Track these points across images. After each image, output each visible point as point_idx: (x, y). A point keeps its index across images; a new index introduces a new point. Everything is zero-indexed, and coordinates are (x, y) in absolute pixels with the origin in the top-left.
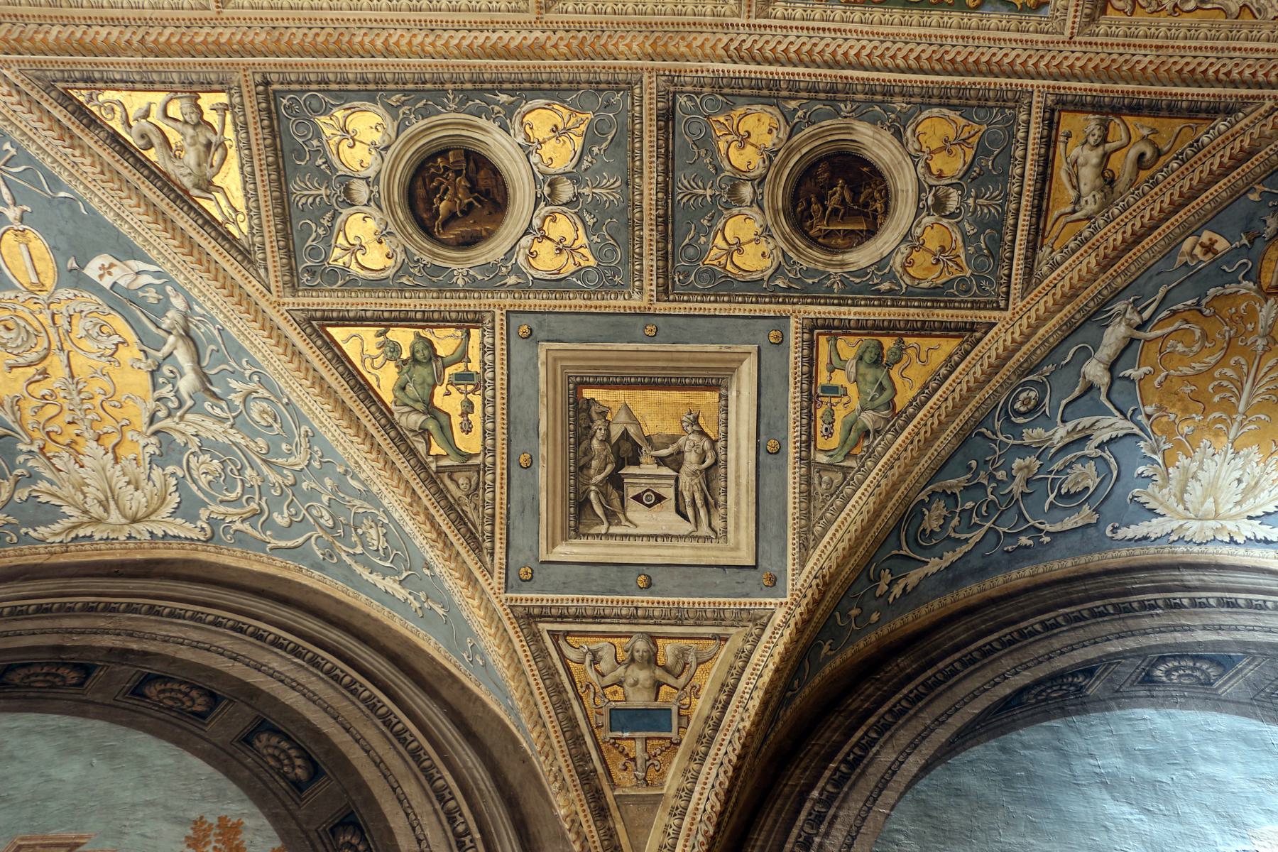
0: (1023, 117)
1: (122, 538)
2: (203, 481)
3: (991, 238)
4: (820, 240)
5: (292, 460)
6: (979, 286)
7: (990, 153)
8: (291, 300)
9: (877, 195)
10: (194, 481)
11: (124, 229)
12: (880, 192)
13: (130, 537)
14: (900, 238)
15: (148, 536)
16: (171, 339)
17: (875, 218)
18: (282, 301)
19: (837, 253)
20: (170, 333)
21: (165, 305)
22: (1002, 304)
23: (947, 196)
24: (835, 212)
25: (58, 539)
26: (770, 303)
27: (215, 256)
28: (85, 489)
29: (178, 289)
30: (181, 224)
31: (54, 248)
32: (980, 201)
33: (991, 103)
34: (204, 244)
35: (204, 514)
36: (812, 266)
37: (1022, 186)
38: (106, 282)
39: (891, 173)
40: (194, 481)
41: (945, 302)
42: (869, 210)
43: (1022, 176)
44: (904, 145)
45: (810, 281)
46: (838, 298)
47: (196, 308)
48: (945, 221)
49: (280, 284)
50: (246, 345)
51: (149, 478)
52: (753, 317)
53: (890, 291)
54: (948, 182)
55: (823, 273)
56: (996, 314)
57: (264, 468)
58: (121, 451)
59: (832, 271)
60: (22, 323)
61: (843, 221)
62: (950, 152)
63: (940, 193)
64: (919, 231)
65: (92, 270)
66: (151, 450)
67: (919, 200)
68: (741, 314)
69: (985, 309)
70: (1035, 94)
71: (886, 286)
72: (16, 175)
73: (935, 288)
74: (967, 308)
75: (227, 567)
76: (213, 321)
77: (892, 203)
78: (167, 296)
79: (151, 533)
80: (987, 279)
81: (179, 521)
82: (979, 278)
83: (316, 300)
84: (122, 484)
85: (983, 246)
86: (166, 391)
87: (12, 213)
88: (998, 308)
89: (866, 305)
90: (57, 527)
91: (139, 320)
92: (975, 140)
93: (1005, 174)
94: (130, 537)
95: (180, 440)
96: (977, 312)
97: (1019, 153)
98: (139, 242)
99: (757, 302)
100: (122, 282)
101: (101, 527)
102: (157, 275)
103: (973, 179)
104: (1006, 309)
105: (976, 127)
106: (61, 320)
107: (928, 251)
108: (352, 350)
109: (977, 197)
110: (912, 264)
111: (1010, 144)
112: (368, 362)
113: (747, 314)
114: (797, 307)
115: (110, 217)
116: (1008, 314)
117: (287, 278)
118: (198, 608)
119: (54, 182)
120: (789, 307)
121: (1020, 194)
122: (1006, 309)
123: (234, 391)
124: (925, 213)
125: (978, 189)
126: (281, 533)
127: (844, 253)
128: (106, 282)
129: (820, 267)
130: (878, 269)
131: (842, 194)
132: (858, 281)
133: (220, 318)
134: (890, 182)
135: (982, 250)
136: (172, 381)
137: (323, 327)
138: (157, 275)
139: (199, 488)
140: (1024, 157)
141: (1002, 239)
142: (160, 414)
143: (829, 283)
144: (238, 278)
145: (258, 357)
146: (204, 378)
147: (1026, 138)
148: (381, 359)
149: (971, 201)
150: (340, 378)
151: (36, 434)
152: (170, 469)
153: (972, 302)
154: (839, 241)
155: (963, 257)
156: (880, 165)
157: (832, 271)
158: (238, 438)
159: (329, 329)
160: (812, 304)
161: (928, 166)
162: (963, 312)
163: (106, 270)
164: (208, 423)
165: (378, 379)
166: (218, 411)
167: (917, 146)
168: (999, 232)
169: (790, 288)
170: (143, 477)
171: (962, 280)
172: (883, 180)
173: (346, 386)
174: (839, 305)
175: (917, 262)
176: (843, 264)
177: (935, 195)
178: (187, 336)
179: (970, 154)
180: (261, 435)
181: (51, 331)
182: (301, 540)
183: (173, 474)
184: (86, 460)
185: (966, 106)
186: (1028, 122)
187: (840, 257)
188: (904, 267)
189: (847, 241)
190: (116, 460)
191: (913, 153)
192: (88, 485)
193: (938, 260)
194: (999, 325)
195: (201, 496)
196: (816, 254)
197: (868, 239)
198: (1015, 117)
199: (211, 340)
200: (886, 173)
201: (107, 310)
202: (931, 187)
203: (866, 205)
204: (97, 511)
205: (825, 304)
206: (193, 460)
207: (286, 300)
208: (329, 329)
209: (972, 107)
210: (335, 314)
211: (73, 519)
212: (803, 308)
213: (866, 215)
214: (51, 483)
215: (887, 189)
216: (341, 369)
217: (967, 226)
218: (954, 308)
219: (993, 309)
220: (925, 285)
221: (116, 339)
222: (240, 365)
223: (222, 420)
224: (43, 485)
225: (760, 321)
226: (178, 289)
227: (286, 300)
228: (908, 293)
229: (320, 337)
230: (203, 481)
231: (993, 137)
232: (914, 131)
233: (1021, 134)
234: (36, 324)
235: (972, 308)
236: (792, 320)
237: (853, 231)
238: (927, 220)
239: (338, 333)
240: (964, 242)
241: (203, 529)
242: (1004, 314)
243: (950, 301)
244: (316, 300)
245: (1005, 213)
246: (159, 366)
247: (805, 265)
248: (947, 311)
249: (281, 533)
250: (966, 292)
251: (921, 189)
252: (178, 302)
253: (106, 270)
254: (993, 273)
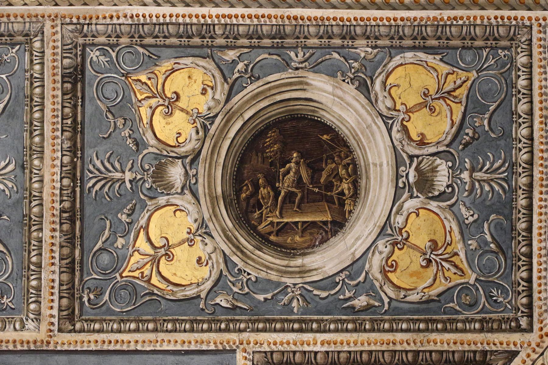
0: (522, 59)
3: (498, 226)
4: (272, 238)
6: (489, 297)
7: (484, 109)
9: (342, 172)
12: (346, 167)
14: (377, 231)
17: (342, 204)
19: (294, 256)
22: (524, 322)
23: (434, 170)
24: (290, 196)
26: (210, 330)
32: (478, 175)
33: (479, 43)
36: (263, 275)
37: (531, 152)
39: (359, 141)
41: (443, 322)
42: (334, 193)
43: (531, 138)
44: (373, 103)
45: (261, 297)
46: (299, 321)
48: (433, 205)
52: (188, 352)
53: (368, 308)
54: (433, 150)
55: (278, 284)
56: (516, 337)
59: (289, 281)
61: (301, 210)
62: (432, 110)
63: (424, 166)
64: (400, 220)
67: (398, 177)
68: (171, 347)
69: (500, 330)
70: (535, 28)
71: (361, 301)
73: (429, 301)
74: (475, 331)
77: (363, 182)
80: (499, 286)
82: (487, 285)
85: (489, 238)
88: (519, 329)
89: (336, 331)
92: (462, 92)
93: (506, 135)
96: (490, 336)
97: (522, 107)
99: (192, 330)
103: (466, 145)
104: (530, 329)
105: (463, 75)
107: (415, 247)
109: (473, 170)
110: (394, 267)
111: (508, 96)
113: (179, 347)
114: (245, 336)
116: (533, 337)
120: (234, 336)
121: (530, 162)
122: (530, 329)
124: (406, 195)
125: (473, 159)
127: (304, 255)
129: (274, 276)
130: (351, 278)
131: (297, 172)
132: (324, 294)
134: (358, 153)
135: (487, 243)
140: (531, 113)
141: (513, 228)
143: (286, 299)
147: (530, 87)
149: (465, 176)
153: (481, 321)
154: (297, 238)
155: (462, 255)
156: (344, 131)
157: (289, 281)
160: (264, 330)
161: (405, 130)
162: (469, 336)
167: (389, 103)
168: (508, 217)
169: (235, 308)
171: (465, 288)
172: (350, 151)
174: (301, 330)
175: (402, 265)
176: (303, 271)
177: (417, 169)
179: (458, 111)
185: (448, 48)
186: (530, 66)
187: (299, 261)
188: (384, 272)
189: (308, 238)
191: (385, 112)
193: (429, 261)
194: (522, 355)
196: (268, 258)
197: (335, 233)
198: (512, 61)
200: (352, 142)
202: (411, 157)
203: (329, 186)
205: (283, 330)
209: (455, 48)
212: (253, 337)
213: (330, 200)
215: (354, 163)
217: (463, 210)
218: (457, 331)
219: (512, 330)
220: (414, 297)
225: (196, 358)
228: (393, 311)
231: (485, 88)
232: (384, 83)
233: (522, 82)
235: (481, 330)
236: (239, 355)
237: (313, 224)
238: (410, 204)
240: (462, 233)
242: (528, 337)
243: (452, 321)
245: (513, 190)
247: (254, 274)
248: (447, 336)
250: (472, 306)
251: (398, 162)
254: (506, 276)
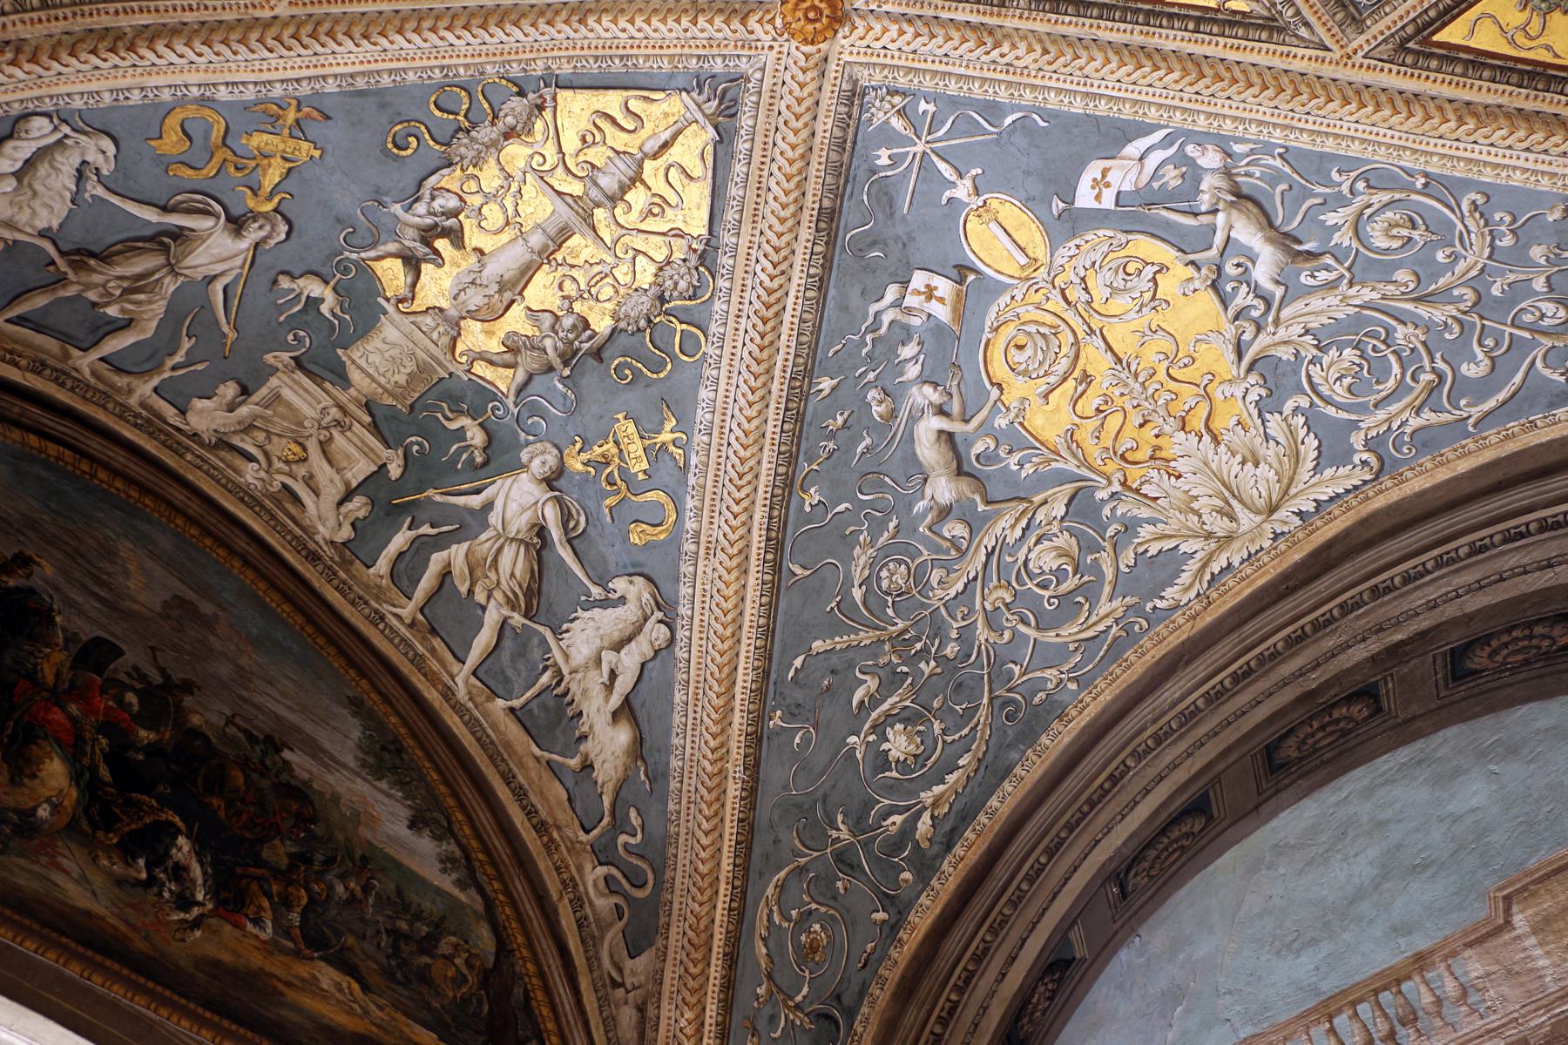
1: (1267, 544)
2: (1340, 392)
5: (1461, 267)
8: (1362, 39)
10: (1327, 401)
11: (1102, 109)
13: (1276, 536)
15: (1297, 521)
16: (1221, 218)
18: (1349, 50)
20: (1215, 212)
21: (1193, 173)
25: (1192, 594)
27: (1232, 56)
28: (1195, 505)
29: (1201, 139)
30: (1170, 46)
31: (1028, 202)
34: (1209, 51)
35: (1357, 440)
38: (1108, 202)
40: (1327, 401)
47: (1238, 148)
49: (1336, 29)
50: (1330, 146)
51: (1267, 437)
57: (1423, 311)
58: (1216, 425)
60: (1032, 328)
65: (1085, 198)
66: (1253, 396)
72: (948, 136)
75: (1421, 495)
76: (1268, 148)
78: (1191, 162)
79: (1300, 514)
81: (1329, 472)
83: (1394, 16)
84: (1236, 469)
86: (1242, 298)
87: (962, 191)
90: (1185, 578)
91: (1169, 224)
94: (1276, 536)
95: (1285, 354)
98: (1127, 113)
100: (1127, 187)
101: (1236, 545)
102: (1167, 142)
106: (1075, 294)
108: (1487, 40)
112: (1520, 39)
115: (1078, 107)
117: (1339, 16)
118: (1435, 552)
119: (992, 110)
123: (1336, 227)
126: (1481, 388)
128: (1108, 202)
133: (1277, 136)
136: (1245, 278)
137: (1426, 41)
138: (1167, 142)
139: (1338, 407)
142: (1247, 337)
144: (1277, 62)
145: (1355, 150)
146: (1285, 241)
148: (1536, 22)
150: (1493, 86)
151: (1111, 467)
152: (1289, 406)
158: (1368, 295)
159: (1436, 38)
163: (1100, 184)
164: (1316, 303)
165: (1548, 48)
166: (1323, 276)
170: (1259, 440)
173: (1509, 88)
178: (1241, 197)
180: (1397, 265)
181: (1070, 316)
182: (1518, 379)
183: (1296, 410)
184: (1180, 466)
190: (1216, 440)
192: (1196, 498)
195: (1343, 415)
199: (1274, 178)
201: (1123, 238)
204: (1220, 526)
206: (1315, 371)
207: (1355, 45)
208: (1436, 38)
210: (1432, 13)
211: (1198, 556)
214: (1153, 522)
216: (1486, 74)
221: (1149, 272)
222: (1330, 183)
223: (1331, 286)
224: (1145, 531)
226: (1201, 139)
227: (1355, 45)
229: (1431, 55)
230: (1340, 392)
234: (1049, 319)
239: (1452, 34)
241: (1364, 463)
244: (1394, 16)
246: (1219, 269)
249: (1481, 388)
252: (1210, 159)
253: (1100, 184)
